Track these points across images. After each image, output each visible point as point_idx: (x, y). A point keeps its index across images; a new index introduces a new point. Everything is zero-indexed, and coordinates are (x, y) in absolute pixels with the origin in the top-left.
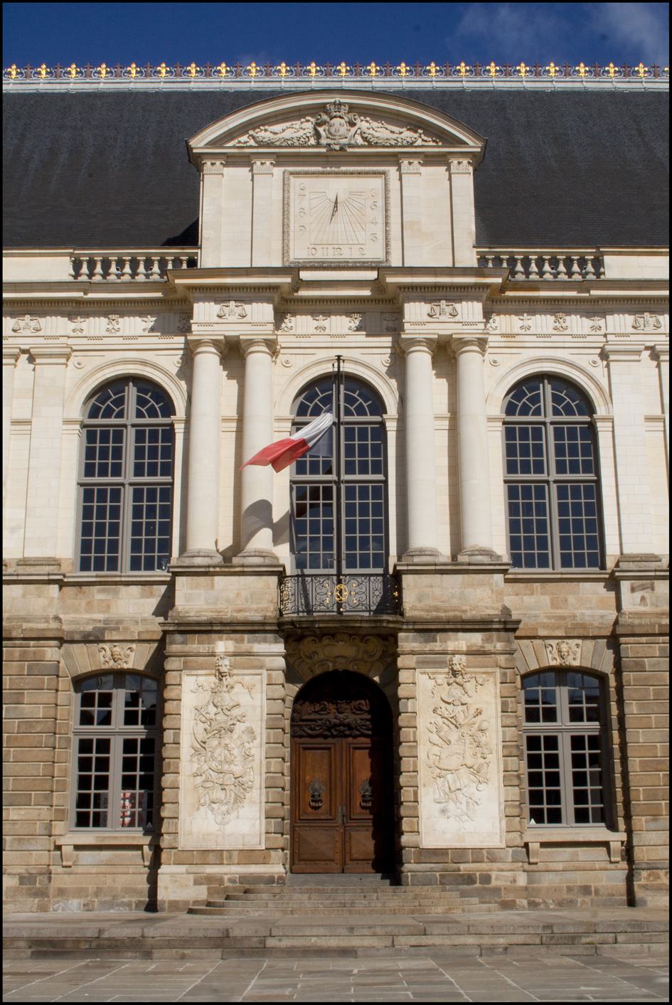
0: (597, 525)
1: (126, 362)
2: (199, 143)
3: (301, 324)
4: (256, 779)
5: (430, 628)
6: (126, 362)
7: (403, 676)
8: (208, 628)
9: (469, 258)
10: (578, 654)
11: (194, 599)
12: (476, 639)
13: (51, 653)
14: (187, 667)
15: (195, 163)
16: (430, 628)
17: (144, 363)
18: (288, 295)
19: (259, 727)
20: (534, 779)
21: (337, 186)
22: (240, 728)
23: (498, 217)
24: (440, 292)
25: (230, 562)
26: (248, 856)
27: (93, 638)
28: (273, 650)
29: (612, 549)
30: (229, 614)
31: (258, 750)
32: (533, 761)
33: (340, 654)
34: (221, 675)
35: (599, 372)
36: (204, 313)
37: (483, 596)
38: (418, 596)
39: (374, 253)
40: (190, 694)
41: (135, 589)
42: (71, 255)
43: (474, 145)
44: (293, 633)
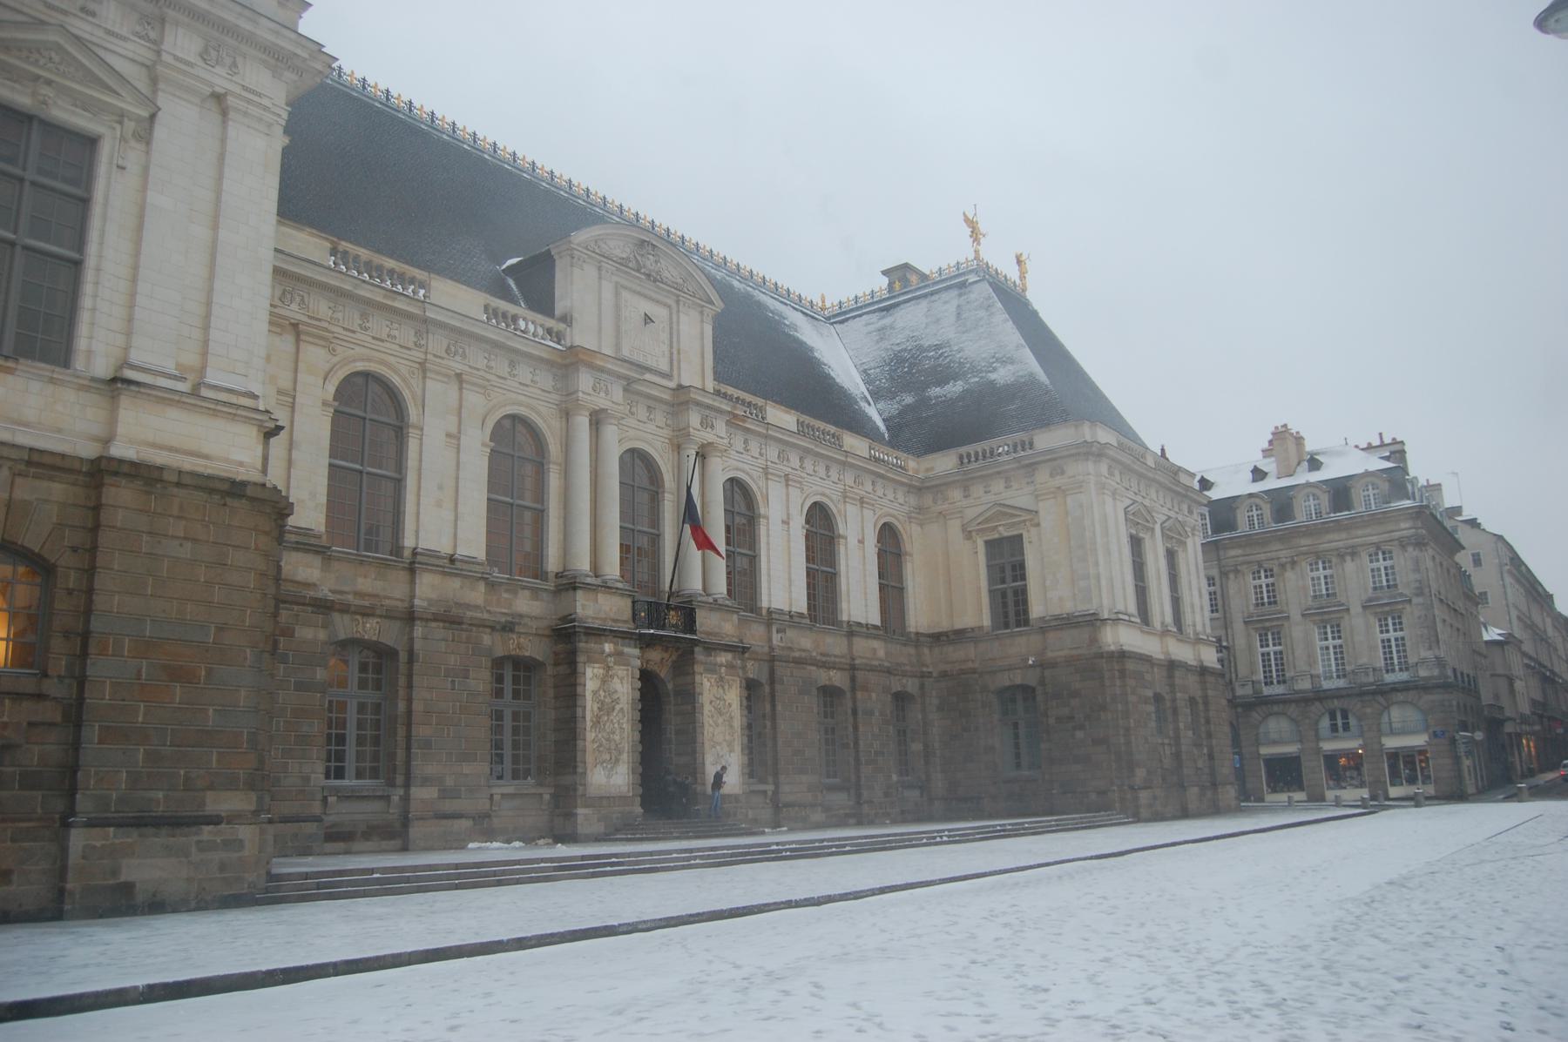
1: (520, 404)
4: (626, 746)
6: (520, 404)
7: (698, 678)
12: (729, 656)
13: (487, 639)
14: (590, 660)
16: (711, 648)
17: (532, 409)
19: (626, 707)
22: (618, 707)
26: (623, 798)
27: (508, 628)
34: (608, 668)
35: (762, 483)
41: (527, 593)
42: (332, 242)
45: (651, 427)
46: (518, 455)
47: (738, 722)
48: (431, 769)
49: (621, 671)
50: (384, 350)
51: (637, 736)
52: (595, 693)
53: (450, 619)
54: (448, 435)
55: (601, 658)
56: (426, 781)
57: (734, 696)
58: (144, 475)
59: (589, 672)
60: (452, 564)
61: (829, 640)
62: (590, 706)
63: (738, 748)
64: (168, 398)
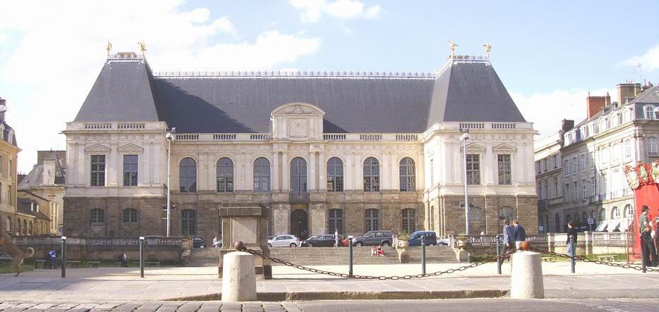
0: (342, 184)
3: (292, 148)
4: (286, 226)
5: (314, 203)
8: (278, 203)
9: (322, 135)
10: (337, 207)
11: (275, 198)
16: (314, 203)
18: (290, 144)
19: (286, 218)
20: (330, 227)
21: (298, 121)
25: (281, 191)
29: (345, 188)
31: (286, 222)
32: (330, 224)
33: (299, 207)
36: (275, 146)
37: (323, 198)
38: (312, 197)
40: (276, 213)
44: (292, 203)
45: (302, 151)
46: (262, 166)
47: (324, 221)
49: (285, 211)
50: (226, 152)
51: (290, 225)
54: (243, 166)
55: (278, 208)
59: (275, 211)
60: (243, 192)
61: (373, 196)
62: (275, 219)
63: (324, 227)
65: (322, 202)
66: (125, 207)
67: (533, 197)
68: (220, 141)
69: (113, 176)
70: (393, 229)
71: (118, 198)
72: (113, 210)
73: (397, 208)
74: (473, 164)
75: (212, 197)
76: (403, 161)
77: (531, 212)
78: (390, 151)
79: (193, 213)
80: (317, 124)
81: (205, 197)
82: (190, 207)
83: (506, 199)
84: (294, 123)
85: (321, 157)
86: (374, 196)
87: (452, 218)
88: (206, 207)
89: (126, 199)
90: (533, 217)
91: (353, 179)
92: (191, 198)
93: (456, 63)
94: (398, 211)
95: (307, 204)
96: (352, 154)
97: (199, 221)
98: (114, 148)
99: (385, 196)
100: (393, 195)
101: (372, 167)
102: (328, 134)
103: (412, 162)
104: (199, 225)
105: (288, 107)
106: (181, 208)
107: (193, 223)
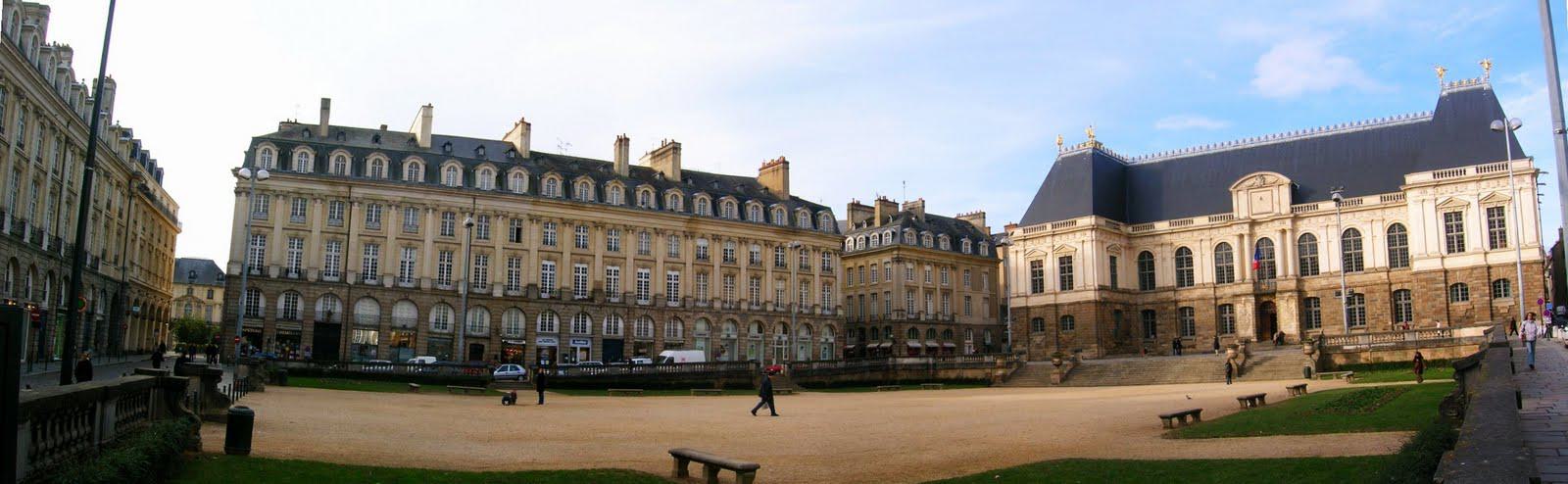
2: (1231, 189)
5: (1280, 292)
12: (1290, 294)
15: (1231, 193)
18: (1253, 224)
19: (1250, 313)
21: (1260, 195)
23: (1298, 196)
24: (1280, 218)
28: (1252, 299)
30: (1244, 292)
31: (1251, 318)
33: (1265, 299)
39: (1269, 209)
40: (1239, 308)
43: (1289, 181)
48: (1201, 333)
52: (1241, 312)
53: (1202, 299)
56: (1200, 335)
57: (1293, 305)
58: (1079, 303)
61: (1356, 277)
64: (1082, 291)
65: (1291, 291)
66: (1062, 314)
67: (1535, 262)
68: (1176, 228)
69: (1052, 279)
70: (1381, 317)
71: (1056, 305)
72: (1050, 319)
73: (1385, 291)
74: (1453, 223)
75: (1171, 294)
76: (1392, 228)
77: (1535, 284)
78: (1371, 220)
79: (1153, 312)
80: (1285, 194)
81: (1164, 295)
82: (1150, 307)
83: (1501, 269)
84: (1256, 196)
85: (1289, 235)
86: (1356, 278)
87: (1428, 300)
88: (1165, 305)
89: (1062, 305)
90: (1536, 290)
91: (1330, 258)
92: (1150, 298)
93: (1444, 93)
94: (1388, 294)
95: (1273, 294)
96: (1325, 225)
97: (1158, 322)
98: (1050, 251)
99: (1372, 277)
100: (1381, 274)
101: (1351, 241)
102: (1297, 206)
103: (1189, 252)
104: (1158, 327)
105: (1253, 180)
106: (1140, 308)
107: (1154, 325)
